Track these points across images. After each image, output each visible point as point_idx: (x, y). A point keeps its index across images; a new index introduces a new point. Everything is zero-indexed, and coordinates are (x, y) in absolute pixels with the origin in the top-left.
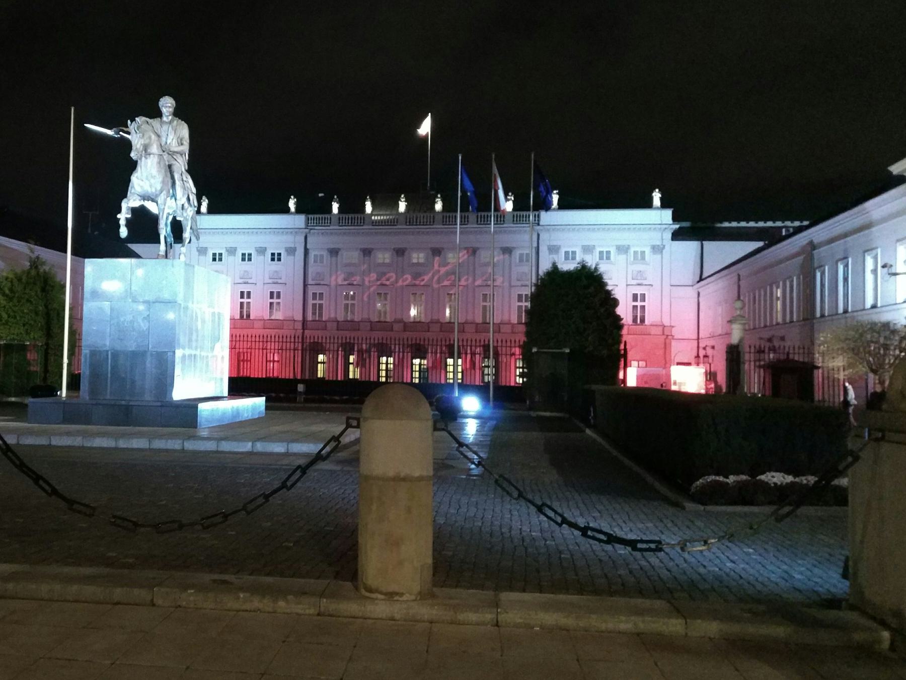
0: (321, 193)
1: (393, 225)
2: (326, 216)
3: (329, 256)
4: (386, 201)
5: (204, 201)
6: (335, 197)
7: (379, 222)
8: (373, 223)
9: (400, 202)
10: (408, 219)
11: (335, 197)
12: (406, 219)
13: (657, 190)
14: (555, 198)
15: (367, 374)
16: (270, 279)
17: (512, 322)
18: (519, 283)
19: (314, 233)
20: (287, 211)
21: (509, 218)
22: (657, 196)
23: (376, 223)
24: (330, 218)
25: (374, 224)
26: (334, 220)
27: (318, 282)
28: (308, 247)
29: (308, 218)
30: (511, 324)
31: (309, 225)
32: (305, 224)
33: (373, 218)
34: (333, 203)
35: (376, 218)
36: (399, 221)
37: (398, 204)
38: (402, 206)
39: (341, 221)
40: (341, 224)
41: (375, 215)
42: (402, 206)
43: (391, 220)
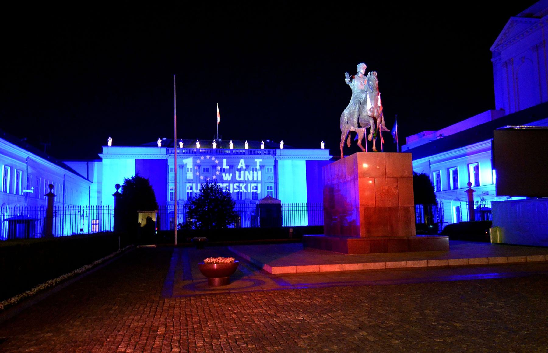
0: (165, 138)
5: (110, 139)
7: (203, 152)
9: (213, 143)
11: (181, 140)
13: (323, 142)
14: (282, 144)
15: (246, 224)
16: (187, 180)
17: (250, 199)
18: (268, 181)
20: (156, 146)
22: (323, 144)
23: (236, 153)
29: (167, 150)
30: (184, 201)
33: (200, 150)
38: (214, 145)
41: (201, 149)
42: (214, 145)
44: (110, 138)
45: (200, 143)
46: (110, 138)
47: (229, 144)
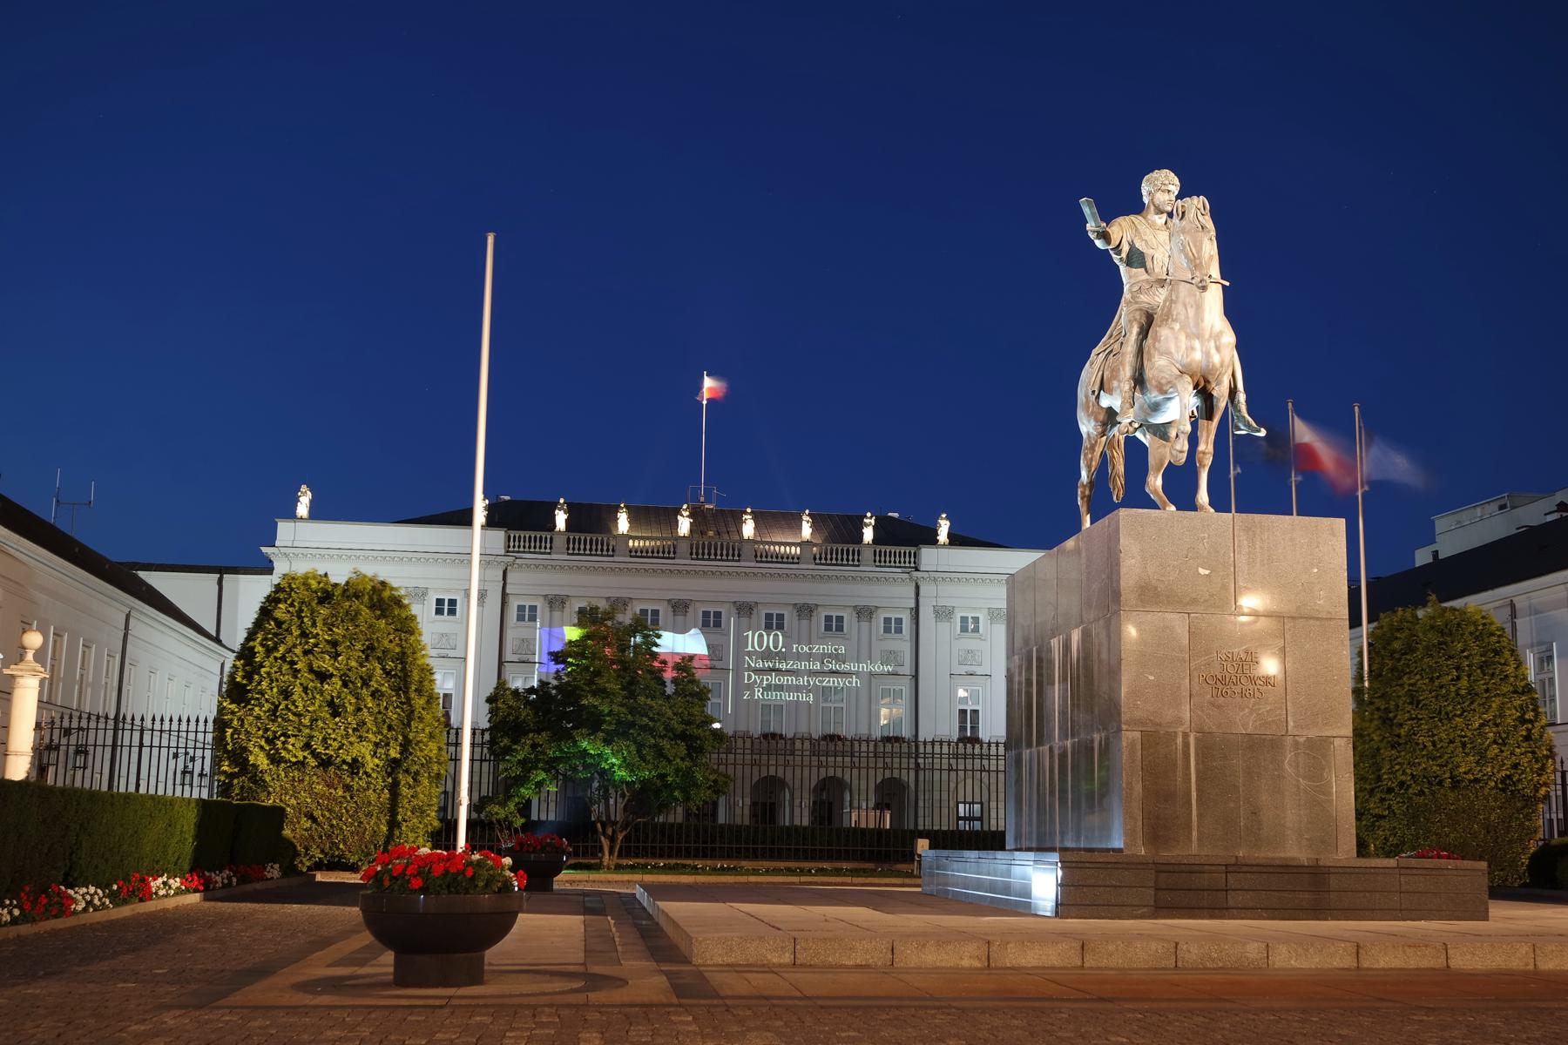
1: (668, 558)
2: (544, 534)
3: (547, 610)
4: (655, 515)
6: (562, 501)
8: (631, 551)
9: (679, 517)
10: (699, 547)
12: (692, 549)
19: (520, 566)
21: (867, 554)
24: (551, 539)
25: (633, 554)
26: (560, 542)
27: (524, 658)
28: (508, 591)
29: (509, 537)
31: (511, 549)
32: (505, 548)
33: (631, 543)
34: (557, 512)
35: (636, 544)
36: (678, 551)
37: (677, 521)
38: (684, 525)
39: (571, 546)
40: (571, 551)
41: (634, 538)
42: (684, 525)
43: (658, 547)
44: (304, 488)
45: (632, 520)
46: (304, 488)
47: (742, 522)
